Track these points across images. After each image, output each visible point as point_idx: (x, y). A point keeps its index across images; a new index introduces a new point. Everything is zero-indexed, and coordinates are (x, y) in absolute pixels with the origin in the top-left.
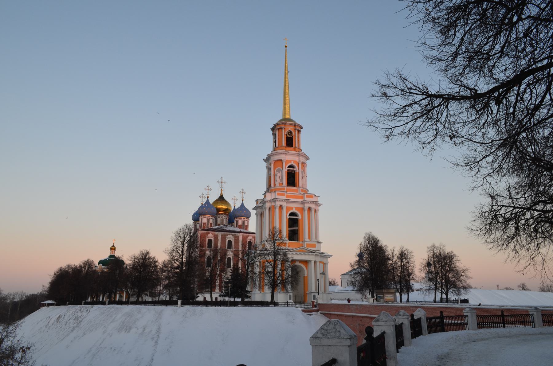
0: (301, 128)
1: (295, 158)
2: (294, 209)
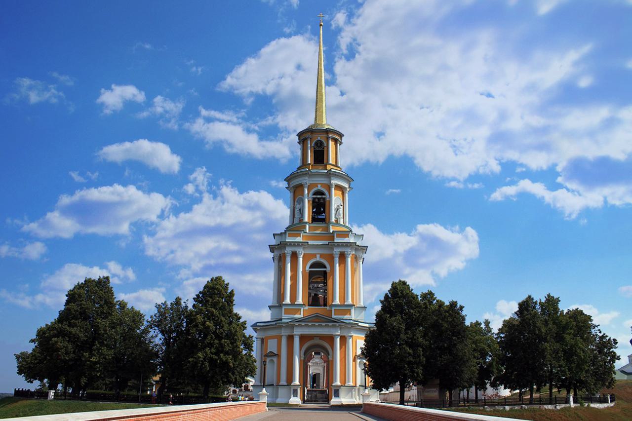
0: (341, 136)
1: (324, 180)
2: (318, 256)
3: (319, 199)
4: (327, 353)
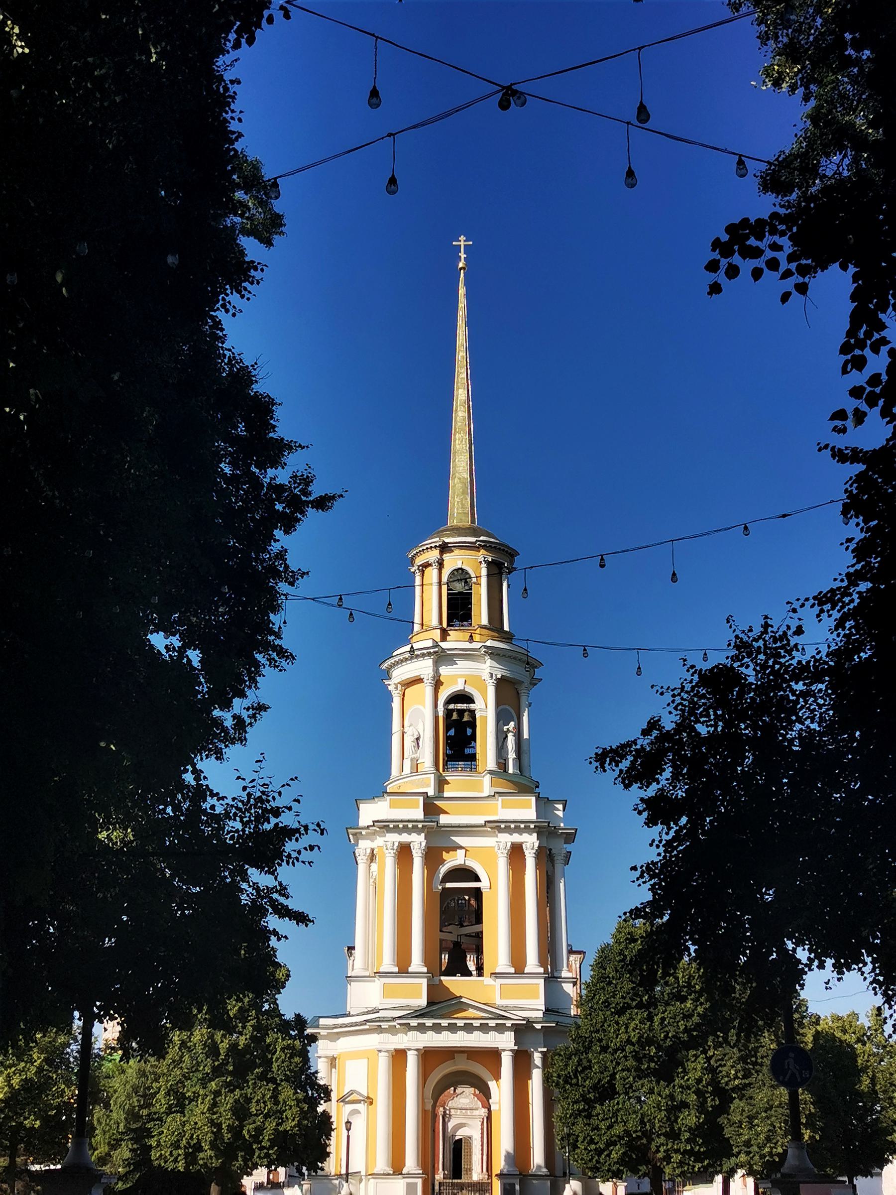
3: (461, 712)
4: (485, 1093)
